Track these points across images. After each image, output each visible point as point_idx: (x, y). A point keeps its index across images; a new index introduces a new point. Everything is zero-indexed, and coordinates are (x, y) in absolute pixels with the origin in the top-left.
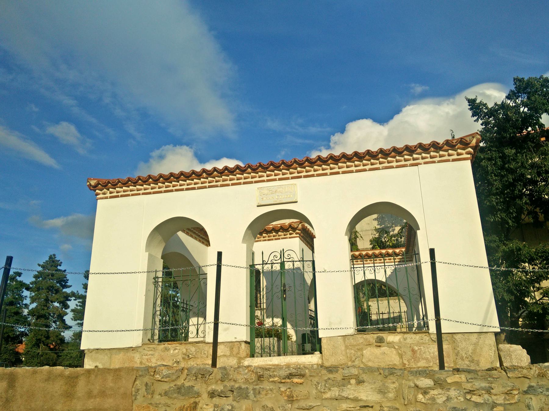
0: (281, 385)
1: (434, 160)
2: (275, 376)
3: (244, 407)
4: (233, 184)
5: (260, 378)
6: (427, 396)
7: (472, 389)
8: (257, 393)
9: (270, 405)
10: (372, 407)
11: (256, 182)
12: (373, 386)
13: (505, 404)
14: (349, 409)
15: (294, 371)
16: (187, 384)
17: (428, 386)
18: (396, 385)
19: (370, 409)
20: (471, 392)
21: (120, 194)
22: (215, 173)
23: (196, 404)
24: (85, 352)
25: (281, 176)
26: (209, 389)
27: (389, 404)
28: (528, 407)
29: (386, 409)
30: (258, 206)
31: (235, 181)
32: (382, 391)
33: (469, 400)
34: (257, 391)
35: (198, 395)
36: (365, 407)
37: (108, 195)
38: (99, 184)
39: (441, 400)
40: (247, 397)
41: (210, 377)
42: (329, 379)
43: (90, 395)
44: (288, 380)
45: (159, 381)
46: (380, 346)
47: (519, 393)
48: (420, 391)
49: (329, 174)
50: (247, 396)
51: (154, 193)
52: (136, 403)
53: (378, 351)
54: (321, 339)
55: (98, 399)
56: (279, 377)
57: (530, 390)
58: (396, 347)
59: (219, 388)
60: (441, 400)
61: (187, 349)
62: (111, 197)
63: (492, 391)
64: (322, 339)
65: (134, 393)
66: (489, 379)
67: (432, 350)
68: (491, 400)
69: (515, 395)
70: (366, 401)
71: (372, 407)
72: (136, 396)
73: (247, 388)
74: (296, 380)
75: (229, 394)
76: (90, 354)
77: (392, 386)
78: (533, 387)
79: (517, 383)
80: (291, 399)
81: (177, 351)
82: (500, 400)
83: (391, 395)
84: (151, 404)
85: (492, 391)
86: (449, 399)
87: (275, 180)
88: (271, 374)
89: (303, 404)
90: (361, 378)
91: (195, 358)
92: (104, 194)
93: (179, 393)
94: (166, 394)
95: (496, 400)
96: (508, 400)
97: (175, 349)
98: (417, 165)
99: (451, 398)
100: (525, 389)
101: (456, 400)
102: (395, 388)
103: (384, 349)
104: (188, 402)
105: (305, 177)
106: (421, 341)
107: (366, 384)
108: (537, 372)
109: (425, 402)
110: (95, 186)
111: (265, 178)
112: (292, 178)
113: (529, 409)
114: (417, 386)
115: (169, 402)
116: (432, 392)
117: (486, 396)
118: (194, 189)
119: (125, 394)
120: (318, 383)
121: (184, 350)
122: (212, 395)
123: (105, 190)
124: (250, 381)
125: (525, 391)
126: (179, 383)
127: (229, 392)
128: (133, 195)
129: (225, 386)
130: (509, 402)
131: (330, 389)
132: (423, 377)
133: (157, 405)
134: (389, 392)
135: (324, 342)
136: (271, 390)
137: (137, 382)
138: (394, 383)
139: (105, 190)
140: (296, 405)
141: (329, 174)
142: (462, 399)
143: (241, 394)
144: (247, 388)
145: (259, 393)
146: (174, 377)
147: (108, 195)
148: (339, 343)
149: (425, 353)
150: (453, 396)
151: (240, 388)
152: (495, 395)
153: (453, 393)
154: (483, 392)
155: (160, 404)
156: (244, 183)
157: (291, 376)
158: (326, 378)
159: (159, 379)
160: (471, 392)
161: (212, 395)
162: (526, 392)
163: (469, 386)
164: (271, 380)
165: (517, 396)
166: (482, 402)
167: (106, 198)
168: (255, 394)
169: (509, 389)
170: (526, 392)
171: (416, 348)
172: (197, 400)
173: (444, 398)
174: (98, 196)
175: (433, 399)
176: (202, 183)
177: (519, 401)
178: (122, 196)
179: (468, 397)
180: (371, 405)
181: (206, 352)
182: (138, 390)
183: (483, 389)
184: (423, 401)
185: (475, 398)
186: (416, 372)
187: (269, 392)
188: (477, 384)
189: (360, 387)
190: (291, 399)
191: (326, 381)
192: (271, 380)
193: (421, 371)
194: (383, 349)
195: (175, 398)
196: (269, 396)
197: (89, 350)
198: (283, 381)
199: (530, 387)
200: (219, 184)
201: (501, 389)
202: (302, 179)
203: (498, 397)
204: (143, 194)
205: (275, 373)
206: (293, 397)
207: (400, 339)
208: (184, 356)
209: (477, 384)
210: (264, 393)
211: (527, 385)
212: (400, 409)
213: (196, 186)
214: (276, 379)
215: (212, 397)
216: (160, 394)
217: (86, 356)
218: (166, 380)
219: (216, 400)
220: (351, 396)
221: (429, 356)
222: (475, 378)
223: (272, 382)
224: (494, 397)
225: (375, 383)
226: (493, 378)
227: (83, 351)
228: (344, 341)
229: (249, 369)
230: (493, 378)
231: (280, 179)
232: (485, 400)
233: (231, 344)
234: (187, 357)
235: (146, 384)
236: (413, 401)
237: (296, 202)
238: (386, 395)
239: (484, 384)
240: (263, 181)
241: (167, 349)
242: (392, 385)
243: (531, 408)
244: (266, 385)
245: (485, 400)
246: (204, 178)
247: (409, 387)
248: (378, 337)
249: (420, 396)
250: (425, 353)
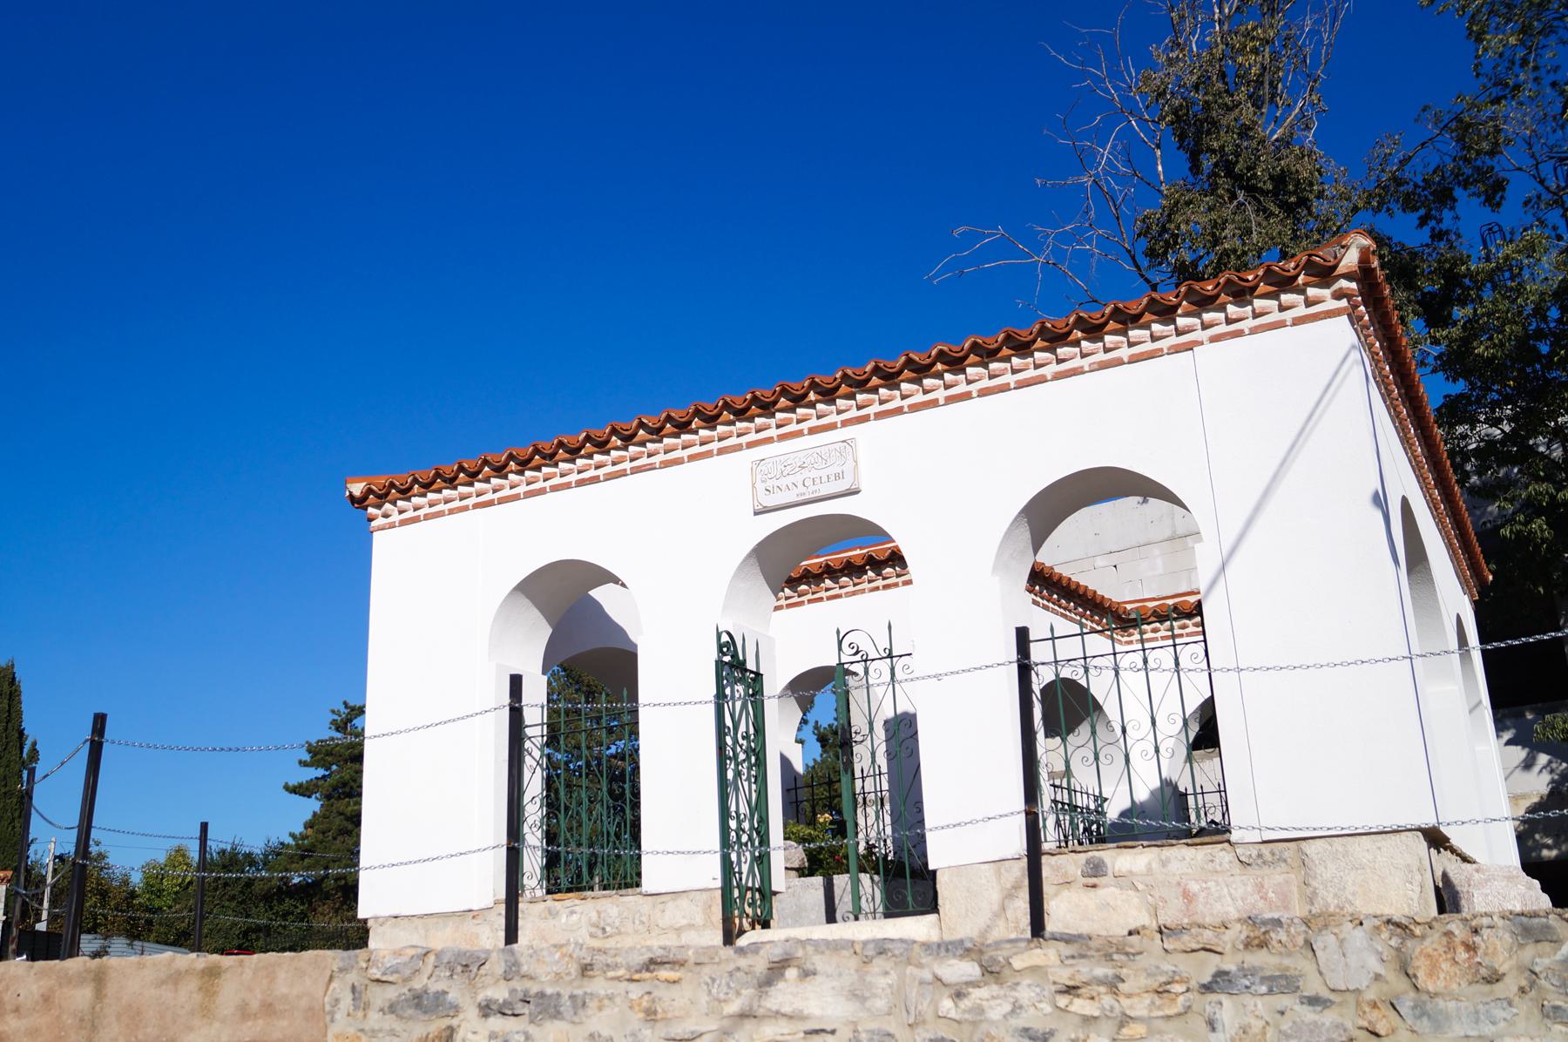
0: (632, 986)
1: (465, 503)
2: (616, 966)
3: (551, 1036)
4: (692, 458)
5: (585, 969)
6: (965, 1003)
7: (1071, 983)
8: (579, 1003)
9: (605, 1033)
10: (833, 1032)
11: (751, 445)
12: (835, 984)
13: (1150, 1018)
14: (779, 1038)
15: (660, 952)
16: (435, 987)
17: (965, 979)
18: (893, 978)
19: (829, 1037)
20: (1071, 990)
21: (421, 512)
22: (641, 432)
23: (451, 1030)
24: (370, 924)
25: (814, 422)
26: (481, 997)
27: (874, 1026)
28: (1212, 1025)
29: (863, 1036)
30: (756, 514)
31: (697, 449)
32: (857, 995)
33: (1064, 1010)
34: (580, 1003)
35: (456, 1009)
36: (817, 1032)
37: (396, 518)
38: (370, 491)
39: (997, 1011)
40: (557, 1015)
41: (482, 971)
42: (738, 969)
43: (244, 1013)
44: (647, 975)
45: (378, 981)
46: (1094, 886)
47: (1188, 990)
48: (947, 992)
49: (942, 401)
50: (559, 1012)
51: (502, 501)
52: (334, 1030)
53: (1090, 899)
54: (934, 872)
55: (261, 1022)
56: (628, 968)
57: (1219, 983)
58: (1140, 887)
59: (500, 993)
60: (997, 1011)
61: (599, 913)
62: (403, 523)
63: (1121, 986)
64: (938, 874)
65: (328, 1008)
66: (1115, 957)
67: (1241, 891)
68: (1117, 1010)
69: (1177, 995)
70: (821, 1018)
71: (833, 1032)
72: (332, 1013)
73: (559, 995)
74: (664, 973)
75: (520, 1008)
76: (380, 930)
77: (883, 982)
78: (1227, 973)
79: (1185, 965)
80: (651, 1015)
81: (575, 917)
82: (1140, 1007)
83: (880, 1004)
84: (362, 1030)
85: (1121, 986)
86: (1017, 1008)
87: (799, 434)
88: (610, 961)
89: (679, 1030)
90: (808, 966)
91: (620, 933)
92: (386, 516)
93: (418, 1006)
94: (392, 1008)
95: (1131, 1007)
96: (1159, 1008)
97: (572, 913)
99: (1021, 1007)
100: (1207, 979)
101: (1032, 1010)
102: (890, 986)
103: (1108, 892)
104: (437, 1026)
105: (880, 416)
106: (1210, 866)
107: (819, 978)
108: (1243, 937)
109: (957, 1017)
110: (364, 498)
111: (773, 432)
112: (845, 423)
113: (1214, 1030)
114: (938, 979)
115: (398, 1026)
116: (977, 994)
117: (1108, 1000)
118: (595, 480)
119: (311, 1009)
120: (714, 980)
121: (594, 916)
122: (486, 1010)
123: (388, 506)
124: (568, 978)
125: (1204, 986)
126: (417, 985)
127: (520, 1004)
128: (451, 512)
129: (513, 991)
130: (1161, 1013)
131: (738, 994)
132: (955, 956)
133: (374, 1033)
134: (875, 996)
135: (941, 880)
136: (611, 998)
137: (333, 985)
138: (887, 973)
139: (388, 506)
140: (662, 1031)
141: (942, 401)
142: (1048, 1008)
143: (545, 1007)
144: (559, 995)
145: (584, 1004)
146: (407, 972)
147: (396, 518)
148: (984, 881)
149: (1219, 899)
150: (1025, 1002)
151: (542, 995)
152: (1129, 996)
153: (1025, 993)
154: (1102, 989)
155: (380, 1030)
156: (721, 452)
157: (652, 964)
158: (731, 967)
159: (378, 976)
160: (1071, 990)
161: (486, 1010)
162: (1207, 988)
163: (1064, 976)
164: (611, 974)
165: (1181, 998)
166: (1096, 1014)
167: (392, 526)
168: (575, 1007)
169: (1163, 979)
170: (1207, 988)
171: (1194, 887)
172: (454, 1022)
173: (1007, 1008)
174: (374, 524)
175: (979, 1010)
176: (614, 464)
177: (1188, 1009)
178: (427, 517)
179: (1062, 1001)
180: (829, 1028)
181: (644, 919)
182: (337, 1000)
183: (1101, 982)
184: (953, 1014)
185: (1080, 1006)
186: (939, 946)
187: (606, 1002)
188: (1084, 970)
189: (811, 986)
190: (651, 1015)
191: (731, 974)
192: (611, 974)
193: (951, 943)
194: (1100, 892)
195: (410, 1018)
196: (606, 1012)
197: (376, 918)
198: (636, 976)
199: (1221, 974)
200: (656, 459)
201: (1143, 981)
202: (470, 512)
203: (1135, 1000)
204: (476, 506)
205: (619, 959)
206: (655, 1012)
207: (1150, 863)
208: (593, 930)
209: (1084, 970)
210: (592, 1004)
211: (1213, 970)
212: (898, 1036)
213: (601, 472)
214: (621, 972)
215: (486, 1016)
216: (381, 1010)
217: (371, 933)
218: (390, 979)
219: (496, 1023)
220: (786, 1009)
221: (1231, 909)
222: (1082, 956)
223: (613, 979)
224: (1125, 1002)
225: (840, 975)
226: (1127, 954)
227: (365, 921)
228: (999, 874)
229: (564, 950)
230: (1127, 954)
231: (812, 431)
232: (1103, 1009)
233: (705, 895)
234: (600, 933)
235: (353, 988)
236: (929, 1016)
237: (857, 492)
238: (868, 1004)
239: (1102, 971)
240: (769, 440)
241: (552, 914)
242: (883, 978)
243: (1218, 1026)
244: (598, 986)
245: (1103, 1009)
246: (617, 448)
247: (921, 983)
248: (1088, 862)
249: (947, 1005)
250: (1219, 899)
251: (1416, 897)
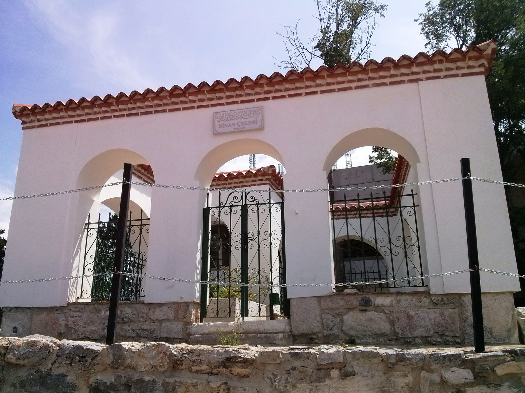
0: (212, 378)
12: (370, 382)
16: (56, 372)
18: (410, 379)
26: (92, 380)
41: (95, 362)
42: (294, 369)
44: (223, 370)
46: (365, 311)
53: (362, 317)
58: (387, 312)
64: (291, 301)
67: (434, 315)
73: (154, 381)
76: (8, 313)
77: (402, 381)
90: (349, 369)
91: (131, 321)
98: (417, 80)
102: (408, 384)
103: (371, 314)
106: (419, 304)
107: (357, 378)
120: (275, 376)
124: (161, 370)
132: (455, 366)
136: (195, 386)
138: (406, 376)
151: (141, 381)
158: (289, 367)
164: (195, 368)
171: (412, 313)
181: (144, 315)
187: (191, 388)
197: (7, 308)
198: (215, 371)
205: (202, 358)
207: (392, 301)
214: (204, 367)
216: (13, 385)
218: (22, 362)
221: (429, 323)
223: (198, 372)
225: (373, 376)
228: (319, 302)
240: (222, 104)
247: (432, 383)
248: (363, 299)
251: (510, 321)
